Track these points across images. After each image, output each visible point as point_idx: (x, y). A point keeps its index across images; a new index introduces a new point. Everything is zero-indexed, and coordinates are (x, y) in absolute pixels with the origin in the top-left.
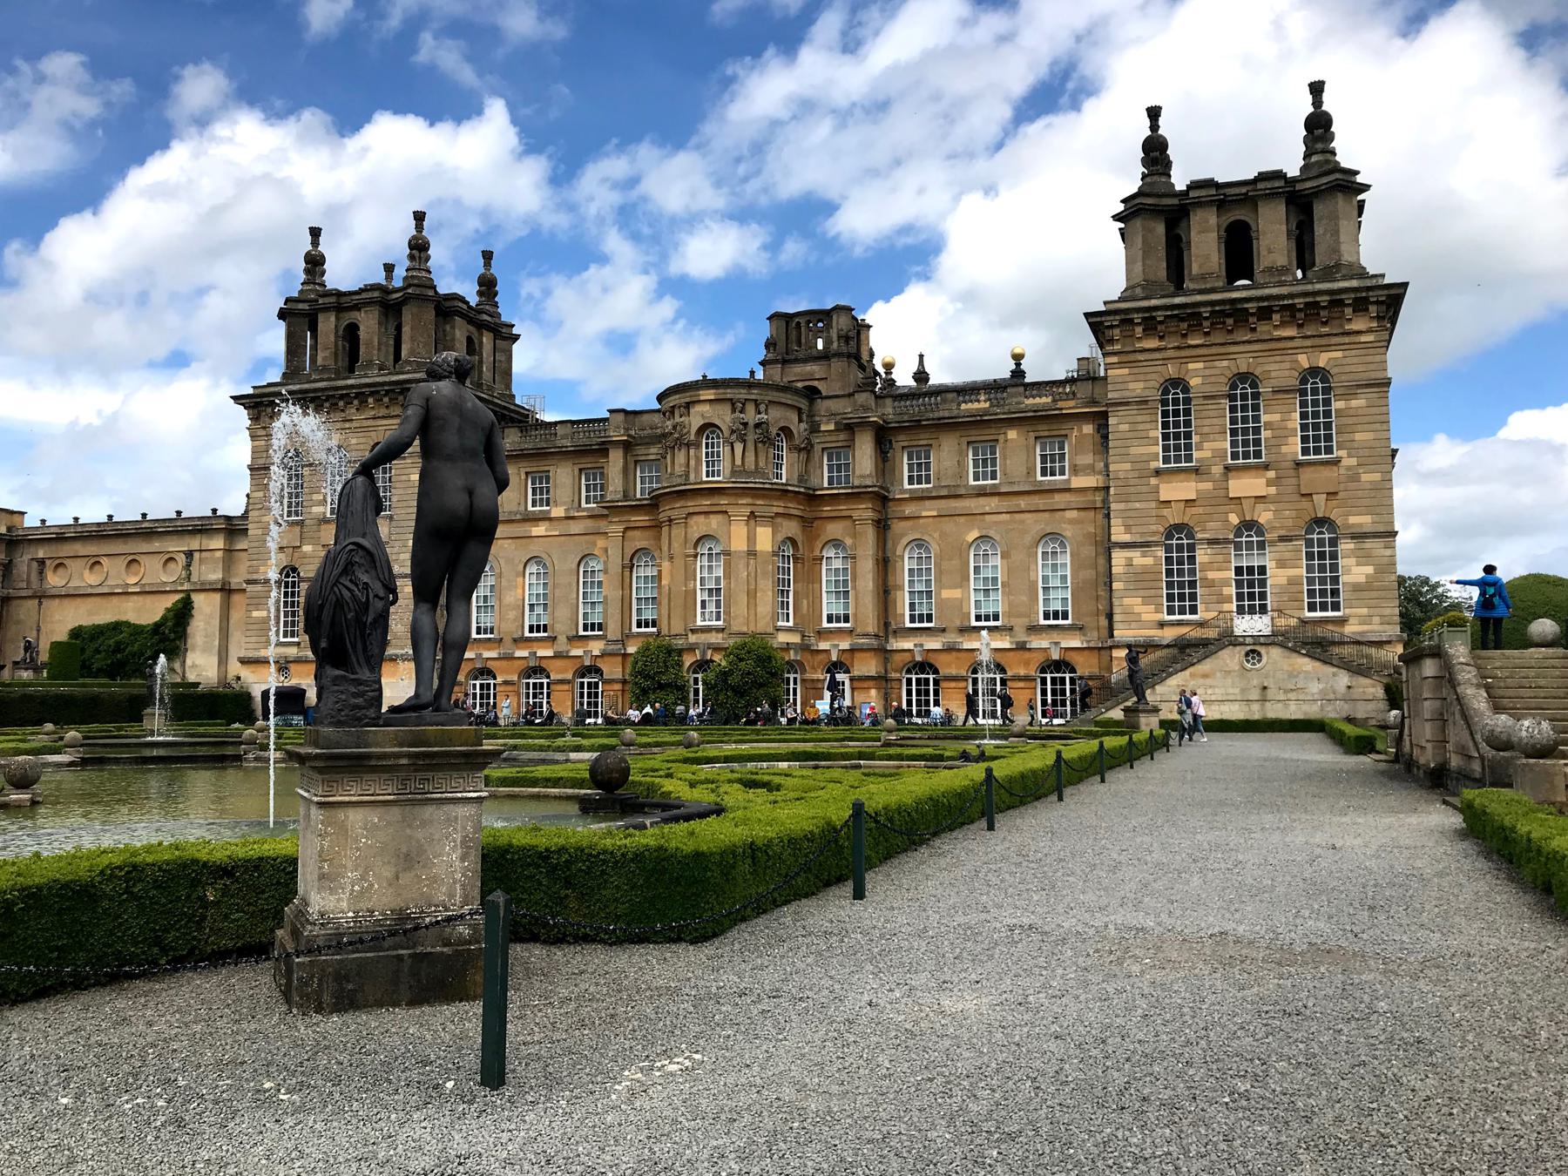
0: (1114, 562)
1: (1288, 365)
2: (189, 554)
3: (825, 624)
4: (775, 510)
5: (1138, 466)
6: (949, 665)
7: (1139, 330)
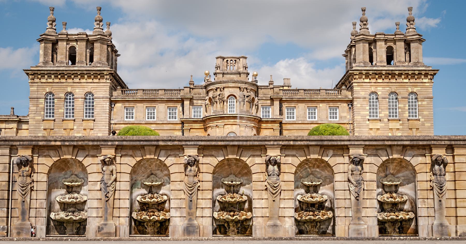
1: (405, 90)
5: (363, 117)
7: (364, 77)
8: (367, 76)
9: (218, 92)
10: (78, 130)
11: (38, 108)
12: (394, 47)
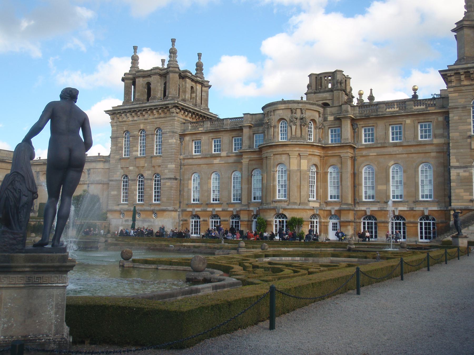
0: (451, 175)
3: (329, 199)
4: (308, 153)
7: (463, 77)
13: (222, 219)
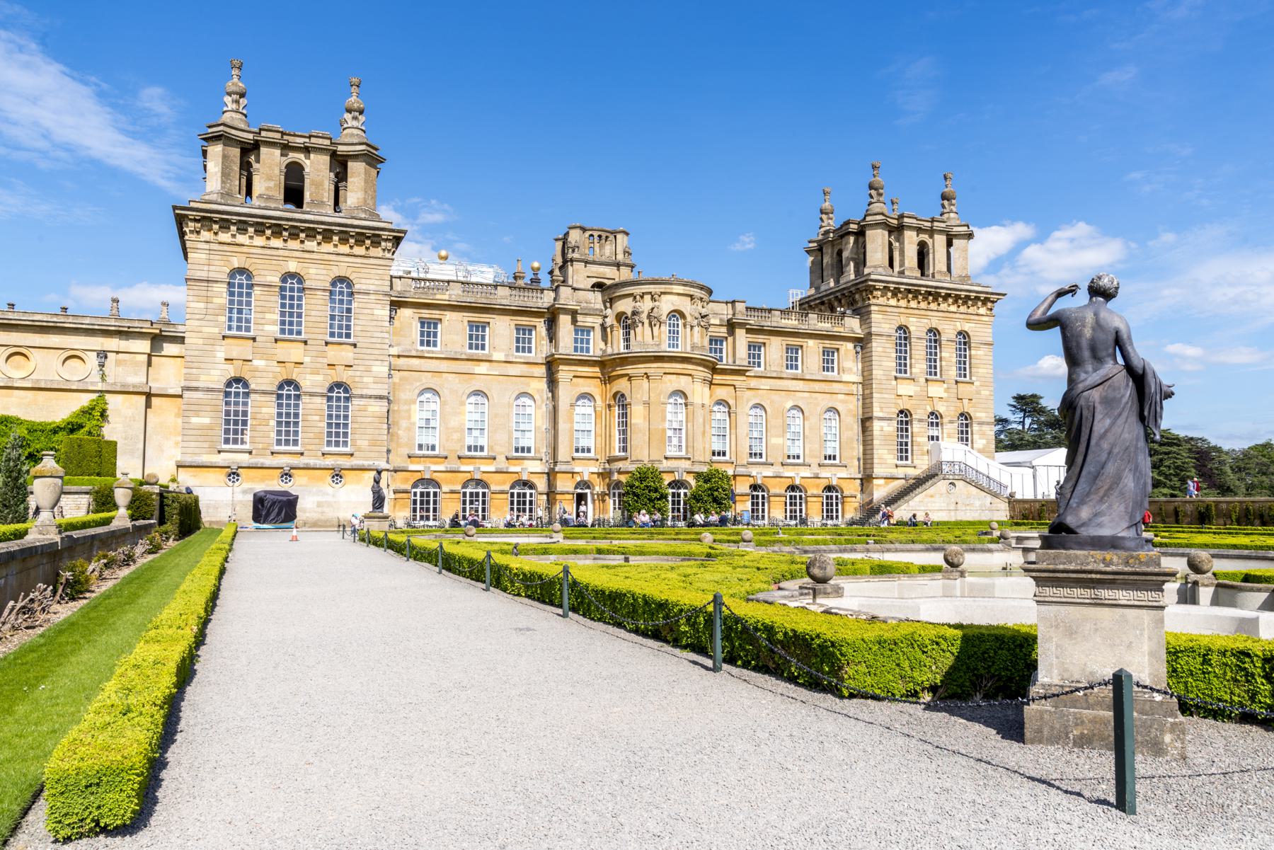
2: (103, 355)
6: (774, 487)
8: (895, 292)
9: (647, 304)
10: (313, 365)
11: (210, 306)
12: (929, 242)
13: (493, 488)
